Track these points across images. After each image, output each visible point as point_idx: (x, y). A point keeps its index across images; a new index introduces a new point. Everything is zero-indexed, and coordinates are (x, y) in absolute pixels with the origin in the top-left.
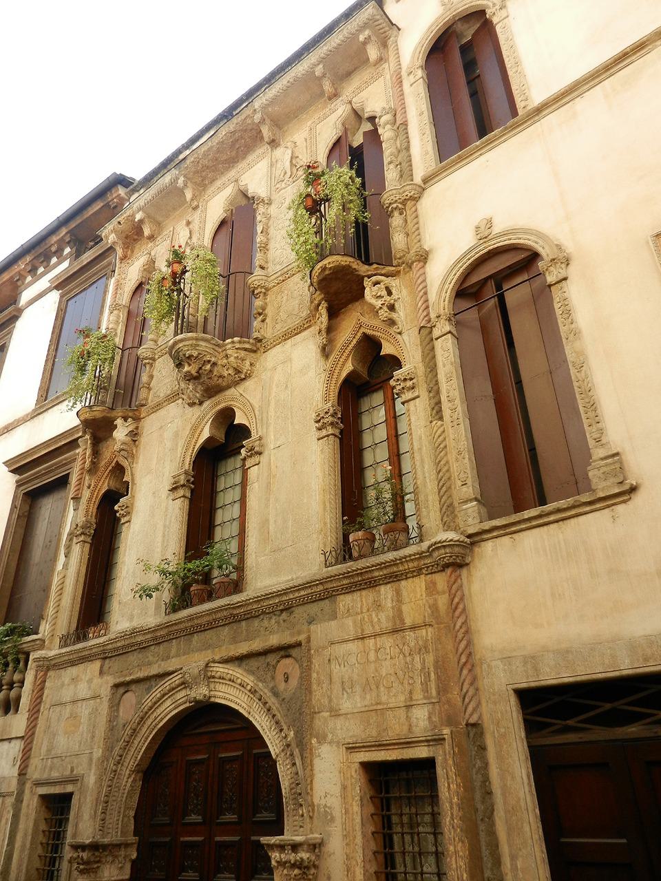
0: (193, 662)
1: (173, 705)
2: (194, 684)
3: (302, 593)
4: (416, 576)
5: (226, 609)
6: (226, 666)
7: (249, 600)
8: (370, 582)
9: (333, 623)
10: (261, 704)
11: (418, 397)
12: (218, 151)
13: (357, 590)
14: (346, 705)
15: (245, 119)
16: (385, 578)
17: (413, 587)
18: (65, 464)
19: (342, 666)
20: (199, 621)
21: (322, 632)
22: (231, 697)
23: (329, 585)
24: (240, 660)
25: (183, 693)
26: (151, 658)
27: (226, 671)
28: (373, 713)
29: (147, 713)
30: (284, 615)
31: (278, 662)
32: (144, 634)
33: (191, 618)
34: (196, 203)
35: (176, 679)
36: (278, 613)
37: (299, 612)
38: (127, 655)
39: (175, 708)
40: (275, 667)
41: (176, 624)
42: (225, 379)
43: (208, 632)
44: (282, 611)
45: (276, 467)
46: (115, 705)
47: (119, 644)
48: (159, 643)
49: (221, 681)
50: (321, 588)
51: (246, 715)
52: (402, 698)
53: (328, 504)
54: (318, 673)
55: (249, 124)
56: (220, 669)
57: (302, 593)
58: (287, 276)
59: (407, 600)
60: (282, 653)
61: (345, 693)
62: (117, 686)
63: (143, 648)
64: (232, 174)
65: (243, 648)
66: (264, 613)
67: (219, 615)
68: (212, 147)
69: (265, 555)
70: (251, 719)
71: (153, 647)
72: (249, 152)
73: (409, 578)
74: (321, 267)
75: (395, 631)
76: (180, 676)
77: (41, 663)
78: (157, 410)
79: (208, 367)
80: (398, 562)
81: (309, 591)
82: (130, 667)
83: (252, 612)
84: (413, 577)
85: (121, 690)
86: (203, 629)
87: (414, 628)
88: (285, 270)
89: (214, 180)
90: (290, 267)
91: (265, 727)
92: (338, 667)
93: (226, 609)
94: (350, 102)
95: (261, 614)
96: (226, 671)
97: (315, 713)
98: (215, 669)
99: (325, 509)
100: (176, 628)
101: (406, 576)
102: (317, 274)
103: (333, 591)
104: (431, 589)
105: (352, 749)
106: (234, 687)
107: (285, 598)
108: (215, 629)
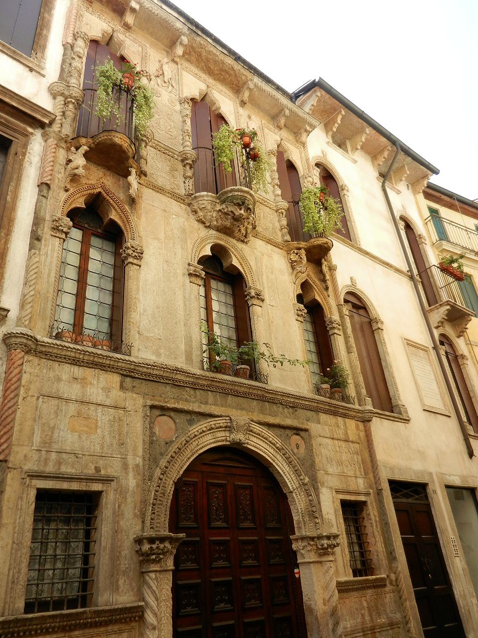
3: (307, 403)
12: (216, 62)
14: (330, 470)
15: (244, 75)
18: (14, 130)
23: (320, 406)
25: (223, 434)
31: (292, 435)
33: (233, 383)
35: (221, 422)
37: (300, 412)
47: (155, 372)
50: (316, 405)
54: (315, 449)
55: (242, 78)
56: (257, 428)
57: (307, 403)
60: (295, 431)
64: (211, 81)
67: (255, 392)
68: (217, 56)
72: (220, 81)
76: (224, 421)
77: (30, 343)
81: (310, 403)
86: (237, 395)
87: (352, 442)
98: (252, 426)
103: (319, 409)
104: (357, 427)
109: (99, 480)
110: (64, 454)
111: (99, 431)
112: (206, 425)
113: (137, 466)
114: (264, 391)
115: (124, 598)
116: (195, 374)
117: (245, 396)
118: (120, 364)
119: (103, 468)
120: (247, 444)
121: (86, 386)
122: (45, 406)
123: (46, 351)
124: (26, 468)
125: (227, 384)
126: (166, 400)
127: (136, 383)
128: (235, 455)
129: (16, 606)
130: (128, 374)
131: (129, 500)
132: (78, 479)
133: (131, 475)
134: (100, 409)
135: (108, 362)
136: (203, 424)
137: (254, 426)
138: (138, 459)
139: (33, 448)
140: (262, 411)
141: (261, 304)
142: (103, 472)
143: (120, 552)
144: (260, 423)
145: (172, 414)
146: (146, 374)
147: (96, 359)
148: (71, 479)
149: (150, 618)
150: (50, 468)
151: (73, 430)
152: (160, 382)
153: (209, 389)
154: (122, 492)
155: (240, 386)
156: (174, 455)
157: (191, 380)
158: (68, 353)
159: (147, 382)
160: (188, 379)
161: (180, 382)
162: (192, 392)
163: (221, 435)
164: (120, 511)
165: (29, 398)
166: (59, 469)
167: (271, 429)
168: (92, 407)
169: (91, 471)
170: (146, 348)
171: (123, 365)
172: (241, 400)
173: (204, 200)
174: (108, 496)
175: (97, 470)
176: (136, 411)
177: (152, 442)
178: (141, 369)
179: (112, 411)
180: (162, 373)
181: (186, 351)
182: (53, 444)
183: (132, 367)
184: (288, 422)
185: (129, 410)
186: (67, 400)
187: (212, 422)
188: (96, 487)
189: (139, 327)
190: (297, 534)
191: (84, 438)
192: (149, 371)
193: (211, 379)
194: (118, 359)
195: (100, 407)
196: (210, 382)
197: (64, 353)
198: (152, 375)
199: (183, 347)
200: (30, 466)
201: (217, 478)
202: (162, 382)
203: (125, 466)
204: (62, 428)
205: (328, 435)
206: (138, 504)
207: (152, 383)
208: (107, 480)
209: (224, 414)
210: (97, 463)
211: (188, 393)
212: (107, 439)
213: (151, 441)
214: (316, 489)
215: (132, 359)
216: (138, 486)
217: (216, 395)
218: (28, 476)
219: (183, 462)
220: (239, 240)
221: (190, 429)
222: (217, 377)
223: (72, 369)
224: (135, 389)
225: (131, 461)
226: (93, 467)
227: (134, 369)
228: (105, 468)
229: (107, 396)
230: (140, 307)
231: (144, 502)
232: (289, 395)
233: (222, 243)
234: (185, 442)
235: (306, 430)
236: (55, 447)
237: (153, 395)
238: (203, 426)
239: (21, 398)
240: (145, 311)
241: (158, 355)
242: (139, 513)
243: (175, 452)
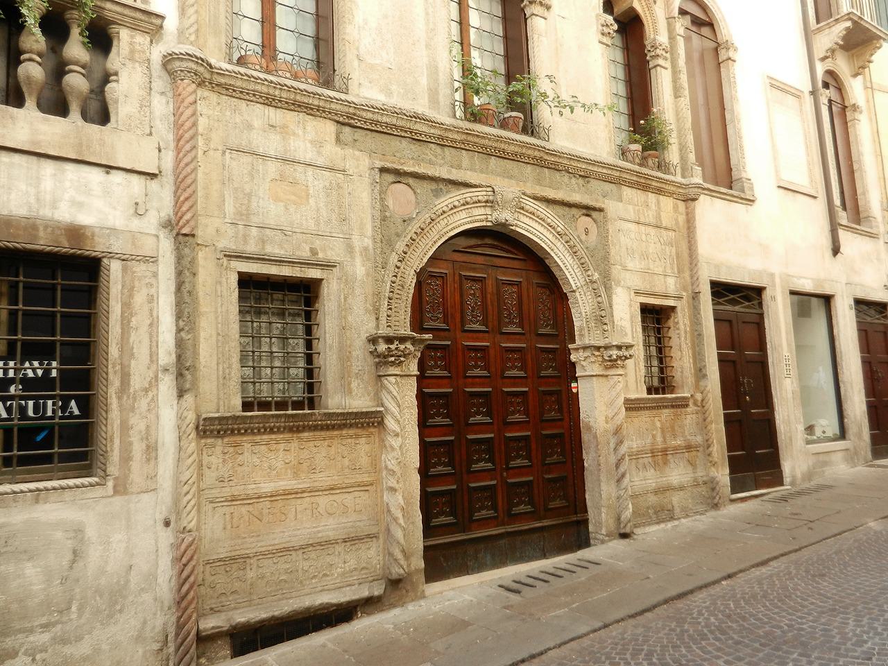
1: (469, 219)
3: (605, 171)
14: (630, 265)
20: (506, 147)
23: (624, 175)
25: (482, 211)
33: (499, 139)
35: (481, 194)
37: (594, 184)
47: (385, 119)
50: (618, 174)
56: (531, 204)
57: (605, 171)
60: (584, 211)
65: (551, 194)
67: (530, 152)
77: (201, 69)
81: (610, 172)
86: (503, 156)
87: (666, 229)
98: (524, 201)
104: (676, 208)
107: (590, 168)
109: (317, 265)
110: (268, 230)
111: (312, 201)
112: (458, 198)
113: (366, 249)
115: (360, 402)
118: (333, 106)
119: (321, 250)
121: (287, 137)
122: (234, 164)
123: (226, 84)
124: (220, 245)
125: (489, 139)
127: (359, 134)
128: (500, 239)
129: (232, 403)
130: (347, 121)
131: (358, 291)
132: (289, 262)
133: (358, 261)
134: (310, 170)
135: (316, 102)
136: (456, 196)
137: (527, 202)
138: (366, 240)
139: (226, 220)
140: (539, 182)
141: (546, 14)
142: (321, 255)
143: (350, 352)
144: (535, 198)
145: (411, 181)
146: (373, 122)
147: (298, 98)
148: (280, 262)
149: (390, 423)
150: (252, 248)
151: (277, 199)
153: (463, 146)
154: (348, 281)
155: (509, 144)
156: (414, 237)
157: (437, 132)
158: (258, 87)
159: (375, 134)
160: (432, 131)
162: (439, 150)
164: (347, 305)
165: (211, 153)
166: (263, 248)
168: (300, 168)
169: (305, 253)
170: (370, 82)
171: (338, 107)
174: (331, 286)
175: (314, 252)
177: (384, 219)
178: (364, 114)
179: (327, 174)
181: (429, 89)
182: (252, 216)
183: (351, 110)
184: (576, 198)
185: (351, 173)
186: (264, 157)
187: (467, 194)
188: (314, 273)
189: (358, 49)
190: (578, 342)
191: (292, 209)
194: (330, 97)
195: (310, 169)
196: (464, 137)
197: (252, 86)
198: (377, 123)
199: (424, 81)
200: (226, 243)
201: (474, 270)
203: (350, 249)
204: (261, 195)
205: (633, 219)
206: (370, 297)
208: (328, 266)
210: (312, 244)
211: (432, 151)
212: (324, 212)
213: (384, 218)
214: (608, 289)
215: (350, 98)
216: (368, 275)
218: (225, 256)
219: (428, 247)
223: (266, 111)
224: (357, 144)
225: (357, 242)
226: (308, 249)
227: (354, 114)
228: (324, 251)
229: (319, 153)
230: (359, 18)
231: (377, 295)
232: (579, 159)
235: (601, 210)
236: (255, 220)
239: (200, 153)
241: (389, 93)
242: (371, 308)
243: (416, 233)
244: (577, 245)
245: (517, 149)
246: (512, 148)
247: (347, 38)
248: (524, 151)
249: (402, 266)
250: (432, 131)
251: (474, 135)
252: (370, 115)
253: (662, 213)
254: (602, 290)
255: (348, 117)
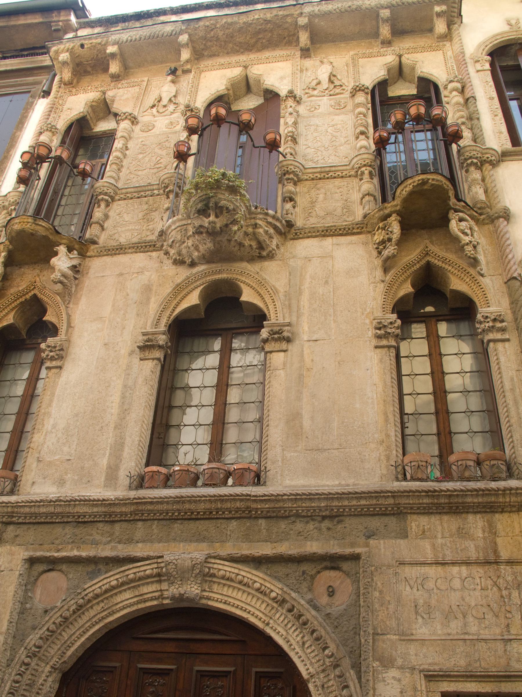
0: (184, 552)
1: (135, 599)
2: (179, 579)
4: (514, 512)
5: (241, 500)
6: (235, 565)
7: (282, 496)
8: (457, 507)
9: (402, 542)
10: (292, 618)
11: (508, 340)
12: (240, 30)
13: (437, 513)
14: (422, 630)
15: (287, 16)
16: (477, 507)
17: (509, 521)
19: (415, 590)
20: (193, 507)
21: (384, 549)
22: (237, 603)
23: (404, 501)
24: (258, 562)
25: (154, 587)
26: (98, 537)
27: (236, 571)
28: (461, 643)
29: (89, 601)
30: (327, 523)
31: (319, 572)
32: (93, 505)
33: (179, 500)
34: (189, 67)
35: (148, 569)
36: (319, 519)
37: (350, 523)
38: (52, 526)
39: (138, 602)
40: (313, 577)
41: (151, 503)
42: (242, 249)
43: (202, 522)
44: (324, 518)
45: (312, 360)
46: (28, 584)
47: (43, 510)
48: (113, 522)
49: (228, 583)
50: (391, 501)
51: (260, 625)
52: (498, 631)
53: (391, 416)
54: (381, 592)
55: (287, 22)
58: (327, 176)
59: (503, 534)
60: (328, 564)
61: (419, 617)
62: (32, 561)
63: (81, 522)
64: (243, 58)
66: (298, 515)
67: (228, 505)
68: (236, 23)
69: (296, 451)
70: (268, 630)
71: (101, 525)
72: (268, 48)
73: (506, 512)
74: (423, 179)
75: (488, 563)
76: (155, 566)
78: (115, 254)
79: (235, 228)
80: (500, 492)
81: (374, 502)
82: (57, 542)
83: (280, 511)
84: (510, 512)
85: (42, 567)
86: (193, 517)
87: (510, 562)
88: (327, 169)
89: (214, 55)
90: (333, 169)
91: (295, 645)
92: (408, 588)
93: (241, 500)
94: (400, 56)
95: (292, 516)
96: (236, 571)
97: (378, 634)
98: (215, 566)
99: (387, 420)
100: (149, 507)
101: (503, 509)
102: (415, 184)
103: (405, 508)
105: (431, 677)
106: (249, 594)
107: (336, 503)
108: (214, 521)
112: (117, 576)
114: (248, 500)
116: (104, 500)
117: (209, 516)
120: (209, 598)
125: (168, 503)
126: (60, 547)
127: (20, 531)
130: (9, 519)
137: (220, 567)
140: (247, 538)
145: (64, 567)
146: (31, 515)
152: (56, 523)
153: (137, 517)
155: (195, 502)
159: (36, 526)
160: (95, 510)
161: (85, 516)
162: (107, 528)
163: (149, 589)
167: (264, 567)
170: (44, 478)
172: (202, 525)
173: (172, 231)
176: (12, 570)
178: (22, 510)
180: (52, 509)
181: (109, 467)
183: (9, 510)
184: (313, 547)
187: (131, 571)
189: (39, 453)
192: (33, 510)
193: (135, 501)
198: (40, 515)
199: (104, 462)
201: (160, 661)
202: (58, 523)
207: (41, 526)
209: (152, 554)
211: (96, 533)
213: (23, 609)
217: (151, 526)
220: (252, 260)
221: (86, 586)
222: (146, 496)
224: (18, 539)
227: (13, 512)
230: (49, 424)
233: (224, 276)
234: (74, 607)
235: (356, 558)
237: (41, 542)
238: (112, 579)
240: (54, 426)
241: (61, 482)
244: (305, 612)
245: (208, 506)
246: (202, 507)
247: (32, 445)
248: (219, 506)
249: (34, 663)
250: (95, 510)
251: (145, 503)
252: (27, 510)
253: (499, 540)
254: (352, 674)
255: (9, 516)
